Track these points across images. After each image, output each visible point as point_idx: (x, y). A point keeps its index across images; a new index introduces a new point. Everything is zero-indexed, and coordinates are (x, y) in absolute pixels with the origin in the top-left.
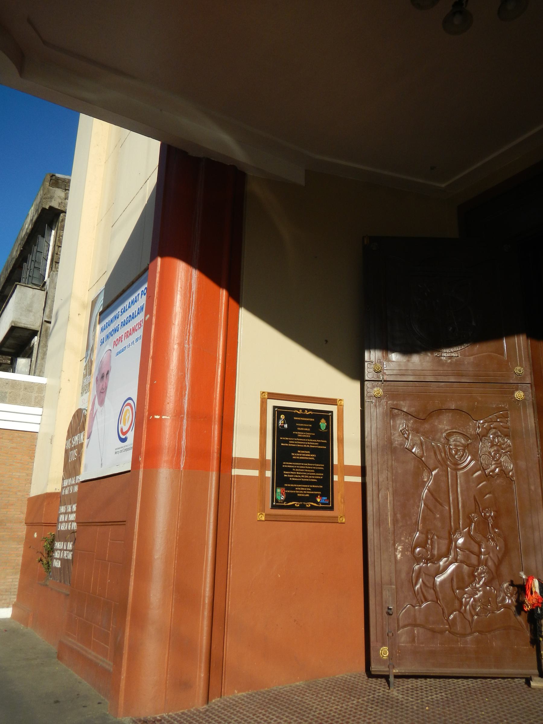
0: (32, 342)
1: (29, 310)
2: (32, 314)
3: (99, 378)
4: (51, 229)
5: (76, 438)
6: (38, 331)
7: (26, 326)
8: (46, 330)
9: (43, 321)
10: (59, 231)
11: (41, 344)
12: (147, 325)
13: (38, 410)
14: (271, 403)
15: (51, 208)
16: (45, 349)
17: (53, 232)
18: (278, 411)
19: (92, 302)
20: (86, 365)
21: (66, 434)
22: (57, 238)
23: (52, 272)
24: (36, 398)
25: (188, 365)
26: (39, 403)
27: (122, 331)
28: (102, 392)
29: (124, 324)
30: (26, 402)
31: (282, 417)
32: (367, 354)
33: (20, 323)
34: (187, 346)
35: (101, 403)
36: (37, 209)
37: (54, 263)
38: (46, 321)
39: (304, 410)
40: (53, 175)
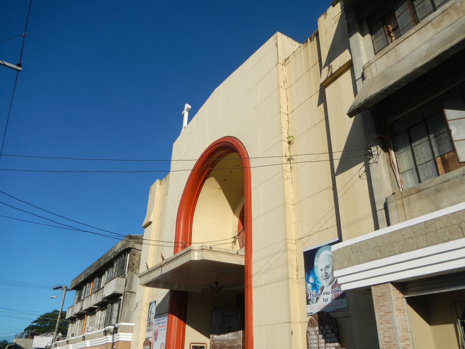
0: (120, 298)
1: (120, 286)
2: (121, 288)
3: (155, 335)
4: (128, 254)
5: (147, 347)
6: (122, 294)
7: (119, 292)
8: (126, 295)
9: (125, 291)
10: (132, 256)
11: (125, 300)
12: (167, 328)
13: (132, 334)
14: (192, 345)
15: (129, 247)
16: (126, 302)
17: (129, 255)
18: (193, 346)
19: (150, 303)
20: (148, 323)
21: (143, 345)
22: (131, 259)
23: (128, 272)
24: (131, 330)
25: (175, 338)
26: (132, 332)
27: (161, 325)
28: (156, 338)
29: (162, 323)
30: (128, 332)
31: (194, 348)
32: (210, 335)
33: (117, 292)
34: (175, 334)
35: (156, 341)
36: (123, 246)
37: (129, 268)
38: (126, 291)
39: (198, 346)
40: (130, 235)
